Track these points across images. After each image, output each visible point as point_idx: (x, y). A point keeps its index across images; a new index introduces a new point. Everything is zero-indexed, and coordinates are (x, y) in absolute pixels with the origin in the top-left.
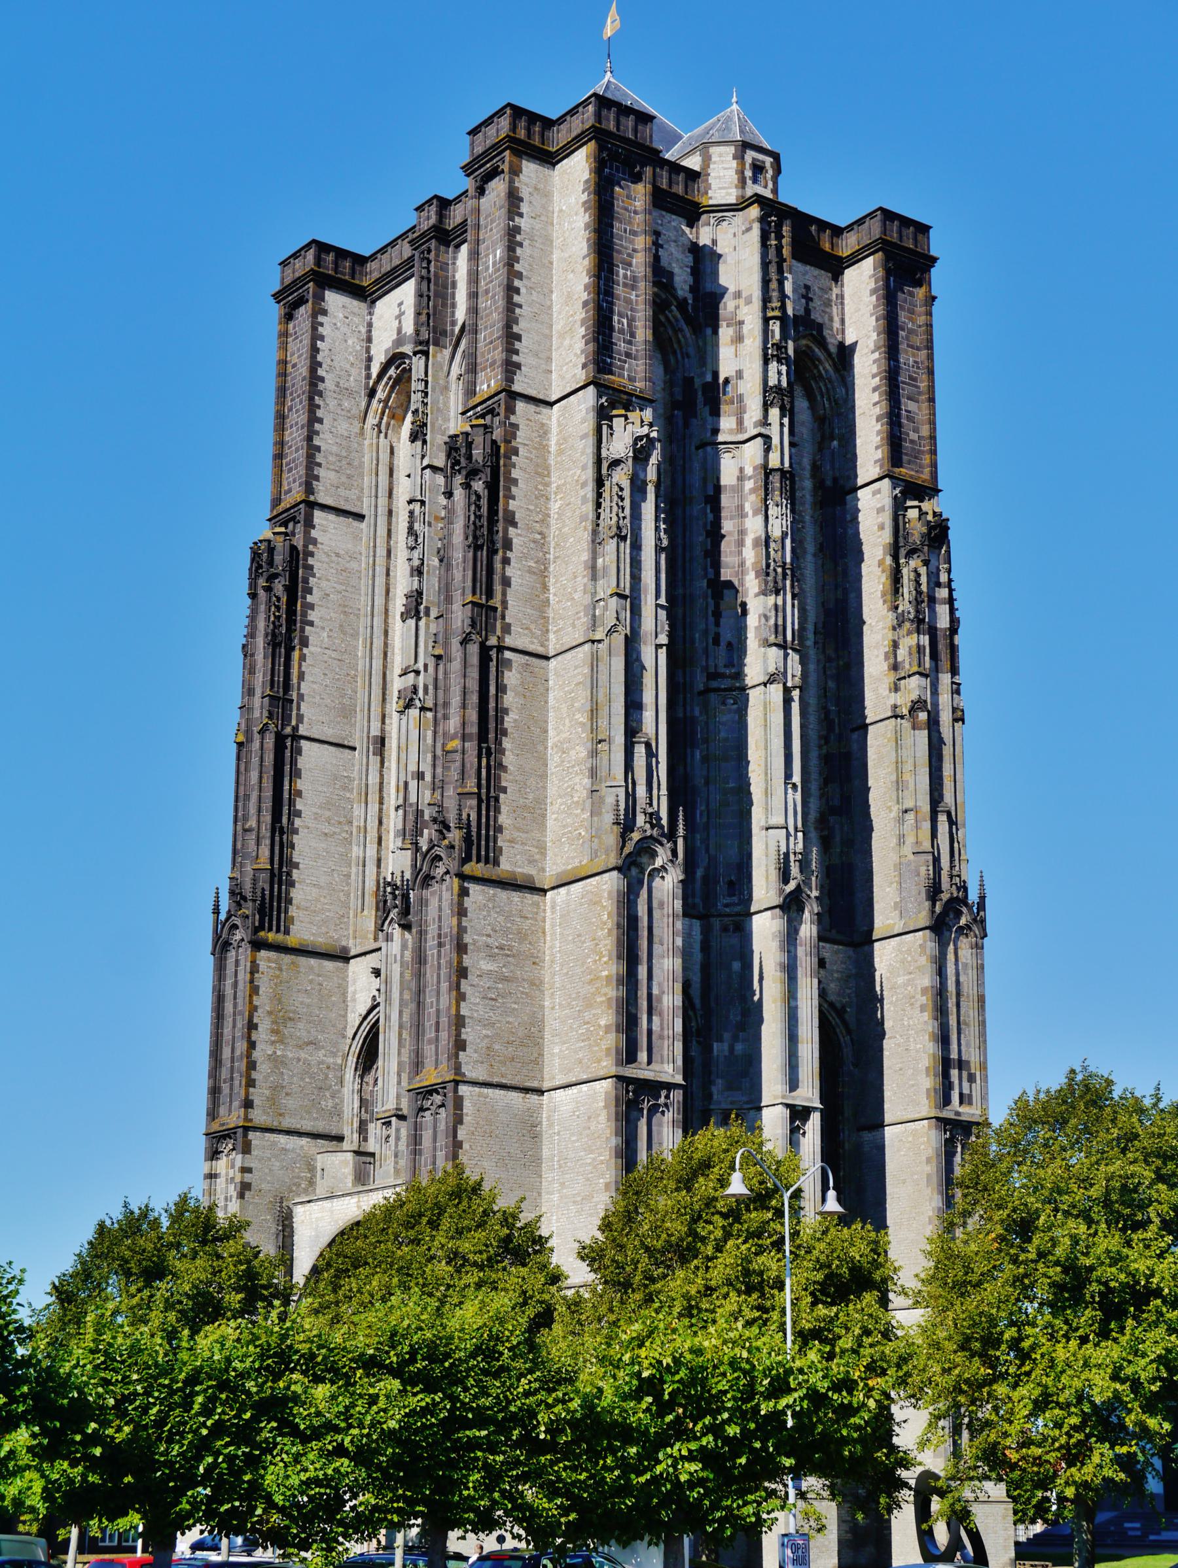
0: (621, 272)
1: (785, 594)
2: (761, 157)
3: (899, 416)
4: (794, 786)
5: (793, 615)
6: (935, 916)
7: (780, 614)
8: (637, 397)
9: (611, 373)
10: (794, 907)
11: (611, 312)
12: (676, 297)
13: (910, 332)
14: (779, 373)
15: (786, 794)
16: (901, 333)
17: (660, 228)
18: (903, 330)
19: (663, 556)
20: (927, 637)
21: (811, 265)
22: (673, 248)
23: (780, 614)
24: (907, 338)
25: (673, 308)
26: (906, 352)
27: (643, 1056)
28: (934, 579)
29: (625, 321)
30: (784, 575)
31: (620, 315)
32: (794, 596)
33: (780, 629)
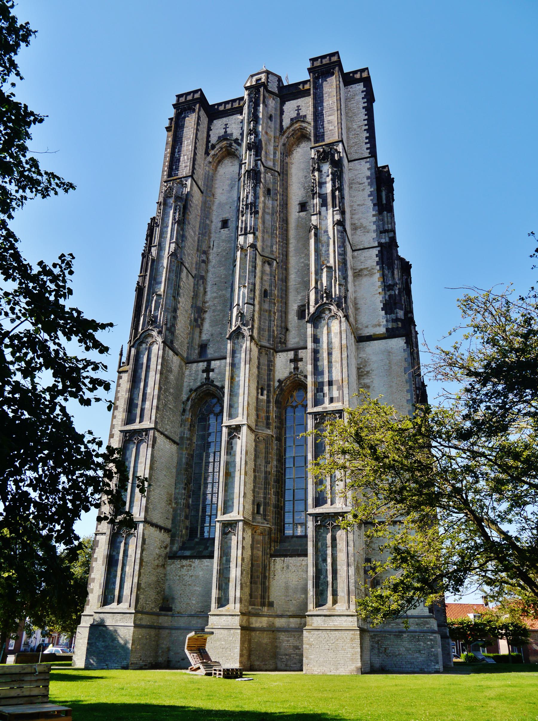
0: (186, 142)
1: (247, 215)
2: (259, 76)
3: (323, 124)
4: (244, 286)
5: (251, 220)
6: (310, 315)
7: (244, 223)
8: (184, 177)
9: (177, 175)
10: (241, 337)
11: (180, 156)
12: (231, 140)
13: (330, 93)
14: (251, 139)
15: (239, 291)
16: (325, 95)
17: (226, 123)
18: (326, 94)
19: (176, 225)
20: (318, 199)
21: (300, 98)
22: (233, 126)
23: (244, 223)
24: (328, 96)
25: (233, 144)
26: (328, 100)
27: (138, 420)
28: (326, 175)
29: (186, 157)
30: (247, 208)
31: (184, 156)
32: (251, 214)
33: (243, 229)
